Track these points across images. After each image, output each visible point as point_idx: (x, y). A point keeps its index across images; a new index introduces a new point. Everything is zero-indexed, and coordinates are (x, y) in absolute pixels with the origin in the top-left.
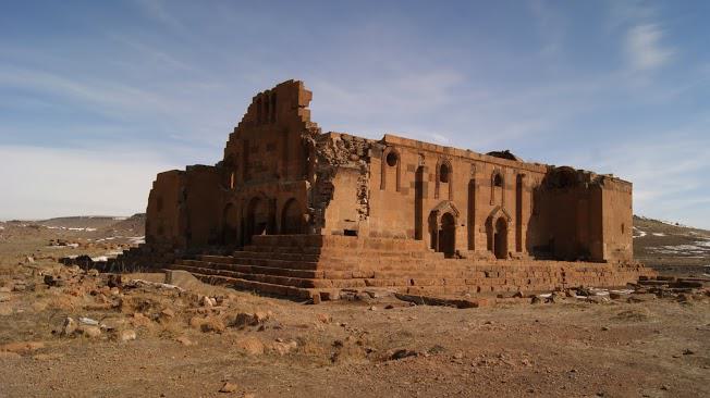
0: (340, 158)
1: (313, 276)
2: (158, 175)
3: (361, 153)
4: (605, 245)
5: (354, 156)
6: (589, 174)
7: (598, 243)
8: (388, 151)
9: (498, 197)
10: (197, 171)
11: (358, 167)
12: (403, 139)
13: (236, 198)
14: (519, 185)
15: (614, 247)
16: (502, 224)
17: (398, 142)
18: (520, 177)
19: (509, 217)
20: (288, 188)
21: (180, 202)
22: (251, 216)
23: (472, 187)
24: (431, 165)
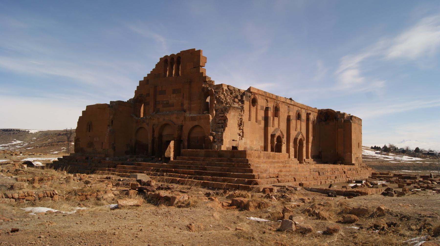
0: (229, 101)
1: (253, 177)
2: (88, 107)
3: (240, 98)
4: (353, 154)
5: (236, 100)
6: (344, 114)
7: (349, 153)
8: (252, 97)
9: (299, 127)
10: (120, 103)
11: (239, 107)
12: (258, 90)
13: (148, 124)
15: (356, 156)
16: (301, 141)
17: (256, 91)
18: (308, 115)
20: (193, 119)
21: (109, 125)
23: (289, 120)
24: (271, 105)
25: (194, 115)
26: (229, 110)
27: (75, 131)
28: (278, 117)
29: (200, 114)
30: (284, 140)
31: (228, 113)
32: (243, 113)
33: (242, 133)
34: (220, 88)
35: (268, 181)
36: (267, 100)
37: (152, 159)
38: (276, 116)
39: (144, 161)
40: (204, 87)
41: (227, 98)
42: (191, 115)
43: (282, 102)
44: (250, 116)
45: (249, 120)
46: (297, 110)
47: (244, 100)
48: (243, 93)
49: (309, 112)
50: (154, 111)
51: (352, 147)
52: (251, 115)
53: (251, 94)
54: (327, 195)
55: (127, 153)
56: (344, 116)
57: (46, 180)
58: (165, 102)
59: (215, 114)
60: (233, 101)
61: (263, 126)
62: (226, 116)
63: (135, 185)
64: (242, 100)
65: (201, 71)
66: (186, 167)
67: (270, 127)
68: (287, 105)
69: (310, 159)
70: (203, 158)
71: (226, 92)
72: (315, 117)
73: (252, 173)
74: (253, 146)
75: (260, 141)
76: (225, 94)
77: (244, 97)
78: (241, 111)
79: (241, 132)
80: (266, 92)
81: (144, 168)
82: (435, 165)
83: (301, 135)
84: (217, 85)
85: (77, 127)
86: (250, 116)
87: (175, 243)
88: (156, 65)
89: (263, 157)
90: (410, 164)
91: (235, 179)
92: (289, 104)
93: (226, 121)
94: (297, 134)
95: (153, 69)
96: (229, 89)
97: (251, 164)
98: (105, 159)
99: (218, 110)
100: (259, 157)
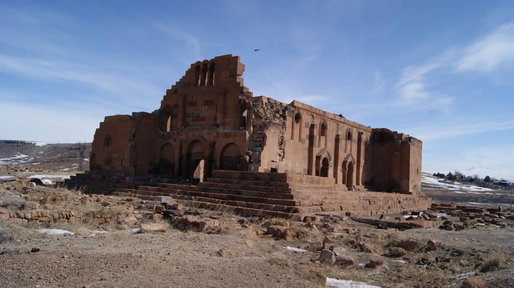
0: (268, 115)
1: (294, 203)
3: (281, 113)
4: (410, 182)
5: (277, 115)
6: (402, 135)
7: (406, 180)
8: (296, 112)
9: (349, 148)
10: (143, 115)
11: (281, 123)
12: (303, 104)
13: (175, 140)
14: (359, 140)
15: (414, 184)
16: (351, 165)
17: (300, 106)
18: (360, 134)
19: (354, 162)
20: (227, 135)
21: (130, 140)
22: (189, 154)
23: (337, 139)
24: (317, 122)
25: (228, 131)
26: (269, 126)
27: (91, 145)
28: (324, 136)
29: (235, 130)
30: (331, 163)
31: (267, 130)
32: (285, 131)
33: (282, 153)
34: (259, 100)
35: (310, 209)
36: (312, 116)
37: (179, 180)
38: (322, 135)
39: (169, 182)
40: (241, 99)
41: (267, 113)
42: (225, 131)
43: (331, 118)
44: (292, 134)
45: (292, 138)
46: (347, 128)
47: (286, 115)
48: (285, 108)
49: (361, 131)
50: (182, 125)
51: (410, 173)
52: (293, 133)
53: (295, 109)
54: (377, 227)
55: (150, 172)
56: (402, 137)
57: (59, 200)
58: (195, 115)
59: (252, 130)
60: (273, 116)
61: (308, 146)
62: (265, 134)
63: (160, 209)
64: (284, 115)
65: (238, 81)
66: (218, 190)
67: (315, 147)
68: (336, 123)
69: (360, 186)
70: (237, 181)
71: (266, 106)
72: (369, 137)
73: (293, 199)
74: (295, 169)
75: (303, 163)
76: (264, 108)
77: (287, 111)
78: (283, 128)
79: (281, 153)
80: (312, 107)
81: (169, 190)
82: (508, 197)
83: (350, 158)
84: (255, 97)
85: (93, 141)
86: (292, 134)
87: (205, 266)
88: (187, 72)
89: (305, 182)
90: (479, 195)
91: (272, 206)
92: (338, 121)
93: (265, 138)
94: (346, 157)
95: (183, 77)
96: (269, 102)
97: (292, 190)
98: (125, 179)
99: (256, 126)
100: (301, 181)
